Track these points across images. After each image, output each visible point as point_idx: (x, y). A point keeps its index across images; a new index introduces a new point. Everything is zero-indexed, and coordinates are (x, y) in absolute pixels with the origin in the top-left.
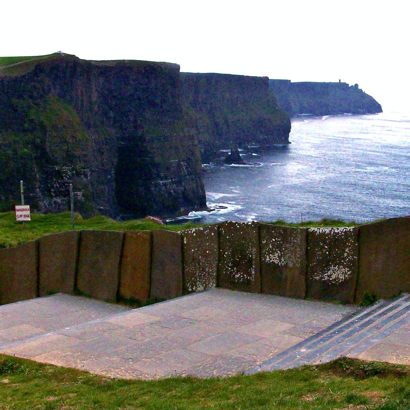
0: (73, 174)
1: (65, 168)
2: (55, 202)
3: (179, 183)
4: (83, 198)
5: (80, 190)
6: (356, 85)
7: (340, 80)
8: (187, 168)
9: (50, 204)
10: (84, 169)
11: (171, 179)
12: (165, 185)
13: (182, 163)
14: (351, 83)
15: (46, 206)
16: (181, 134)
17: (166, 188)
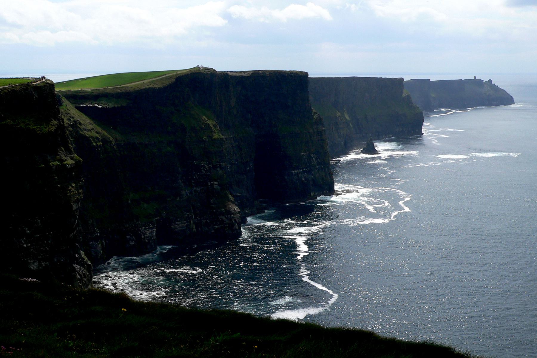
0: (209, 167)
1: (203, 163)
2: (195, 191)
3: (309, 172)
4: (219, 187)
5: (216, 180)
6: (490, 81)
7: (475, 77)
8: (316, 159)
9: (191, 193)
10: (220, 163)
11: (302, 169)
12: (298, 174)
13: (312, 155)
14: (485, 79)
15: (187, 195)
16: (311, 131)
17: (298, 176)
